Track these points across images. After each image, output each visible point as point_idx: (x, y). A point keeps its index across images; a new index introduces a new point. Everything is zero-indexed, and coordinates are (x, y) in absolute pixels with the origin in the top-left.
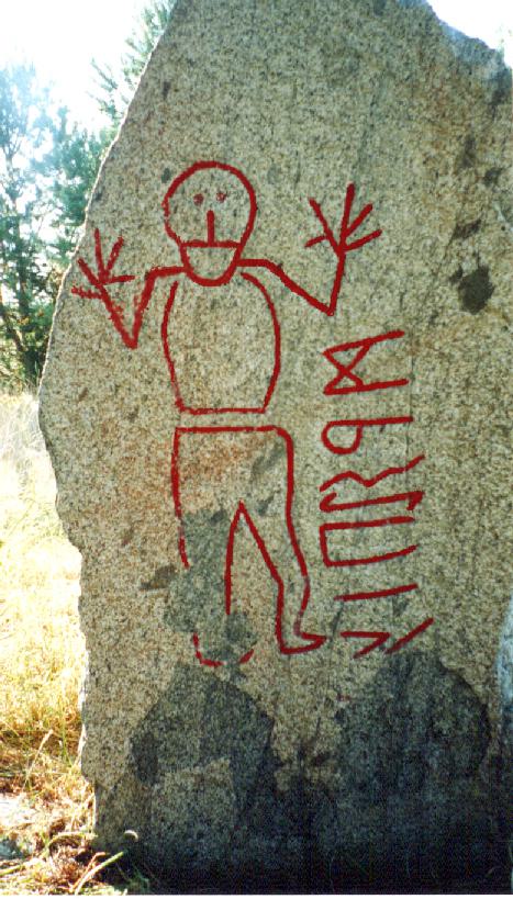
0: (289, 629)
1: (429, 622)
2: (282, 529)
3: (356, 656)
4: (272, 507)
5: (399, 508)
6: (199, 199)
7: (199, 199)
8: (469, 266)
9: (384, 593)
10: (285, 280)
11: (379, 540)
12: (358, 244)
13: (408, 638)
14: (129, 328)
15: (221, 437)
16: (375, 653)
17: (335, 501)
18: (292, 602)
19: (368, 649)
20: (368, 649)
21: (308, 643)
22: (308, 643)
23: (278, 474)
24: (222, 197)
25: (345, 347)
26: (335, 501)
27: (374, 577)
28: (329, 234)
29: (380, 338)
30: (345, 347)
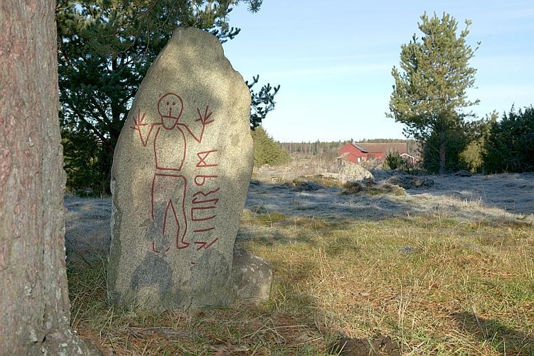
0: (180, 240)
1: (217, 239)
2: (181, 208)
3: (198, 249)
4: (179, 201)
5: (212, 203)
6: (168, 103)
7: (168, 103)
8: (234, 133)
9: (206, 230)
10: (189, 130)
11: (208, 213)
12: (207, 123)
13: (212, 244)
14: (145, 140)
15: (167, 177)
16: (203, 249)
17: (196, 201)
18: (182, 231)
19: (201, 247)
20: (201, 247)
21: (185, 245)
22: (185, 245)
23: (181, 192)
24: (174, 104)
25: (202, 153)
26: (196, 201)
27: (203, 225)
28: (201, 119)
29: (211, 151)
30: (202, 153)
